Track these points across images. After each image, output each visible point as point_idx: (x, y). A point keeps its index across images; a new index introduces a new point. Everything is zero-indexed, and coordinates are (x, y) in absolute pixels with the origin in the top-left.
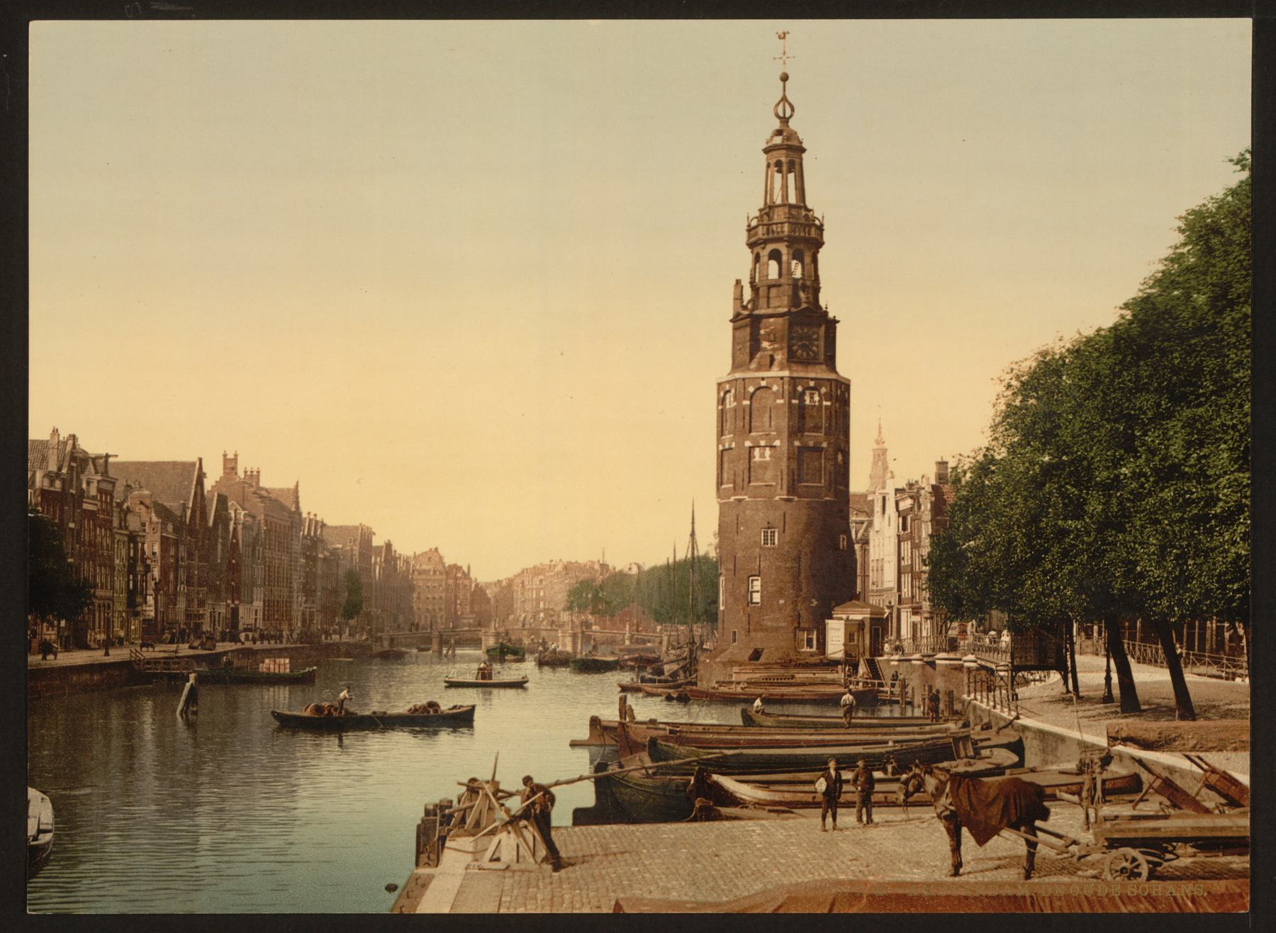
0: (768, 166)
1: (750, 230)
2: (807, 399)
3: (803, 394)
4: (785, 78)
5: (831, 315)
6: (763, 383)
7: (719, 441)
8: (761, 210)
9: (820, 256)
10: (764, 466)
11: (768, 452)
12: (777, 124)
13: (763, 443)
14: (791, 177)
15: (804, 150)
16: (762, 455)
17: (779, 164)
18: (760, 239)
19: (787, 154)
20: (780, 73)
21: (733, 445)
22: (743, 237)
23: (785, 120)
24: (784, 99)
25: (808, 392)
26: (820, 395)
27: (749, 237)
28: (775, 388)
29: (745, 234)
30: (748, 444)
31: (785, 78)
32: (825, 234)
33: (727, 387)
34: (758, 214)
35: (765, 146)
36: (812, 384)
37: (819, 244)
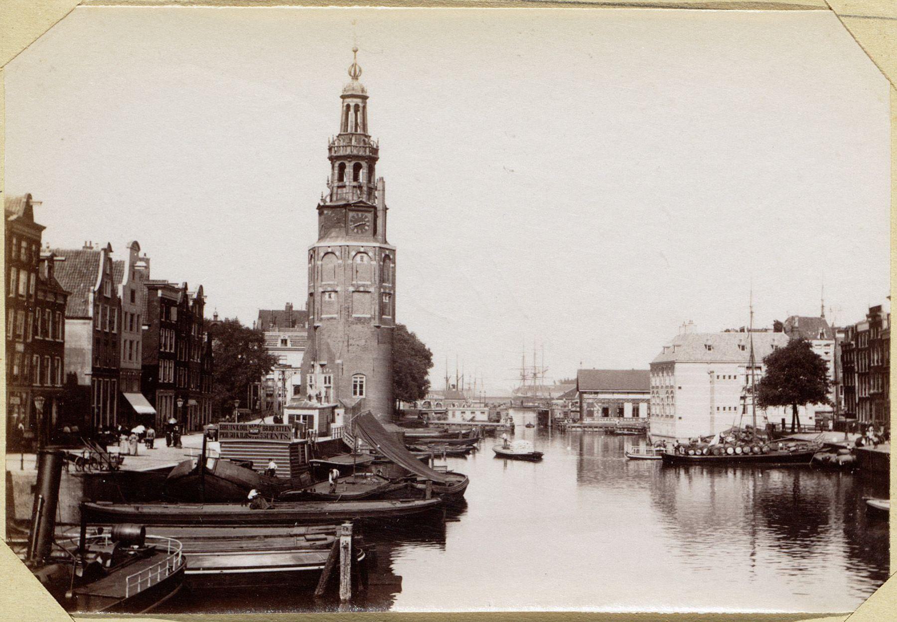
1: (330, 149)
4: (355, 51)
6: (330, 250)
11: (333, 295)
12: (348, 80)
15: (364, 98)
17: (348, 106)
23: (355, 77)
28: (337, 253)
30: (321, 290)
31: (355, 51)
35: (341, 94)
36: (362, 250)
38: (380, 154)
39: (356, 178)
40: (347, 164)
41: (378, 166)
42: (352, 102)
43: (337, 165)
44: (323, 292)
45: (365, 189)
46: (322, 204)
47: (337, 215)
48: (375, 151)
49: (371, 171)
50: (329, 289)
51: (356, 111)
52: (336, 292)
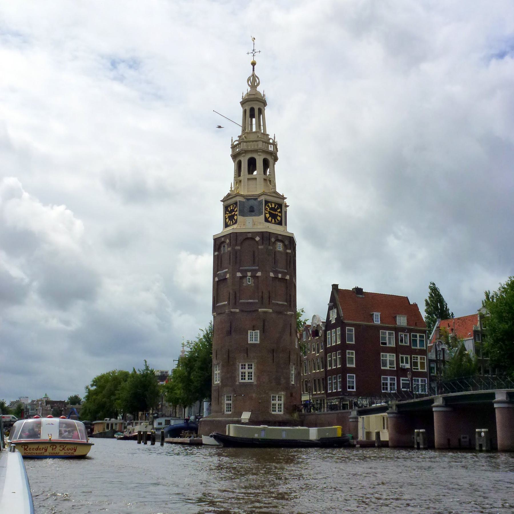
0: (245, 112)
1: (233, 147)
3: (274, 243)
4: (254, 64)
6: (250, 236)
7: (215, 275)
8: (239, 137)
9: (275, 166)
13: (249, 274)
17: (252, 110)
21: (228, 276)
22: (230, 152)
24: (254, 76)
27: (233, 151)
29: (231, 150)
30: (239, 274)
31: (254, 64)
33: (223, 239)
34: (238, 139)
37: (276, 159)
38: (279, 154)
41: (279, 167)
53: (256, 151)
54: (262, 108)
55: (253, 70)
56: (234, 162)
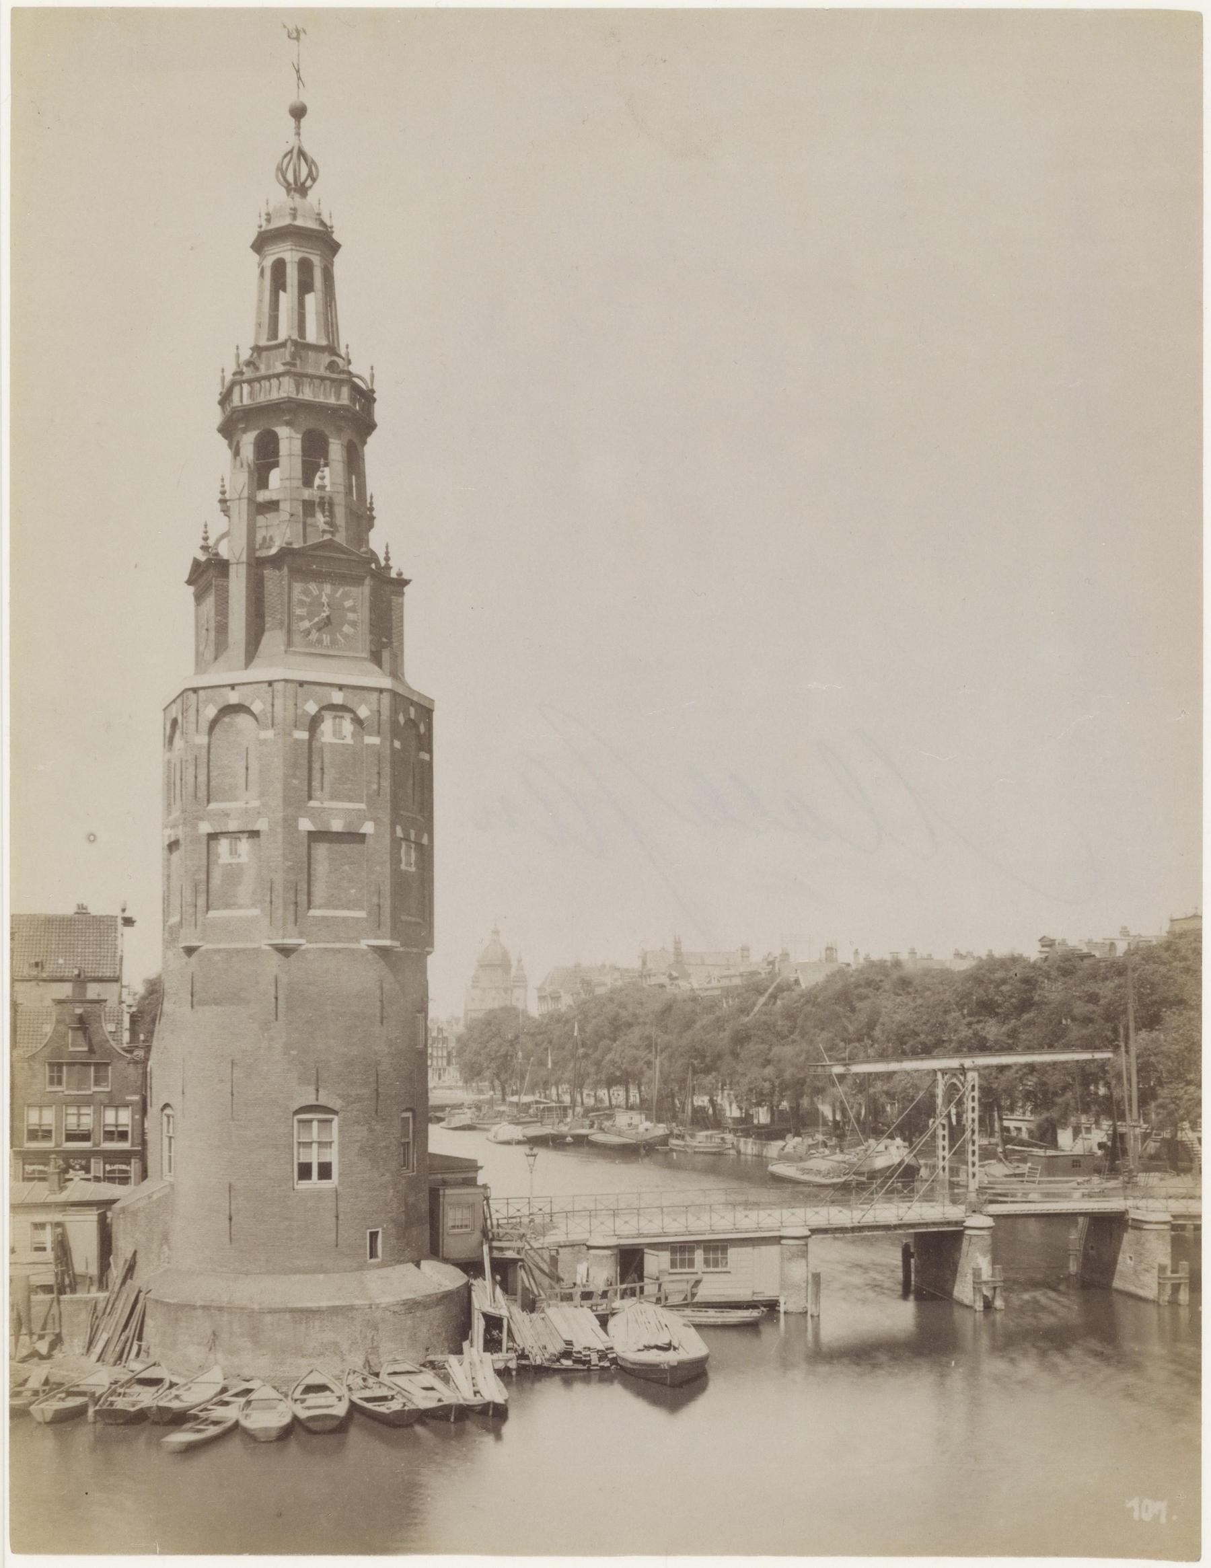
2: (327, 726)
4: (299, 113)
5: (393, 575)
6: (233, 698)
10: (234, 875)
11: (244, 845)
12: (279, 197)
14: (312, 301)
16: (233, 852)
18: (248, 421)
19: (301, 253)
20: (291, 99)
25: (328, 716)
26: (357, 721)
31: (299, 113)
32: (378, 408)
36: (338, 698)
38: (380, 412)
39: (309, 471)
40: (283, 432)
42: (290, 254)
43: (248, 440)
44: (213, 837)
45: (340, 512)
46: (202, 557)
47: (248, 590)
48: (366, 397)
49: (354, 462)
50: (233, 826)
51: (305, 287)
52: (254, 834)
53: (275, 410)
54: (316, 260)
55: (298, 134)
56: (230, 446)
